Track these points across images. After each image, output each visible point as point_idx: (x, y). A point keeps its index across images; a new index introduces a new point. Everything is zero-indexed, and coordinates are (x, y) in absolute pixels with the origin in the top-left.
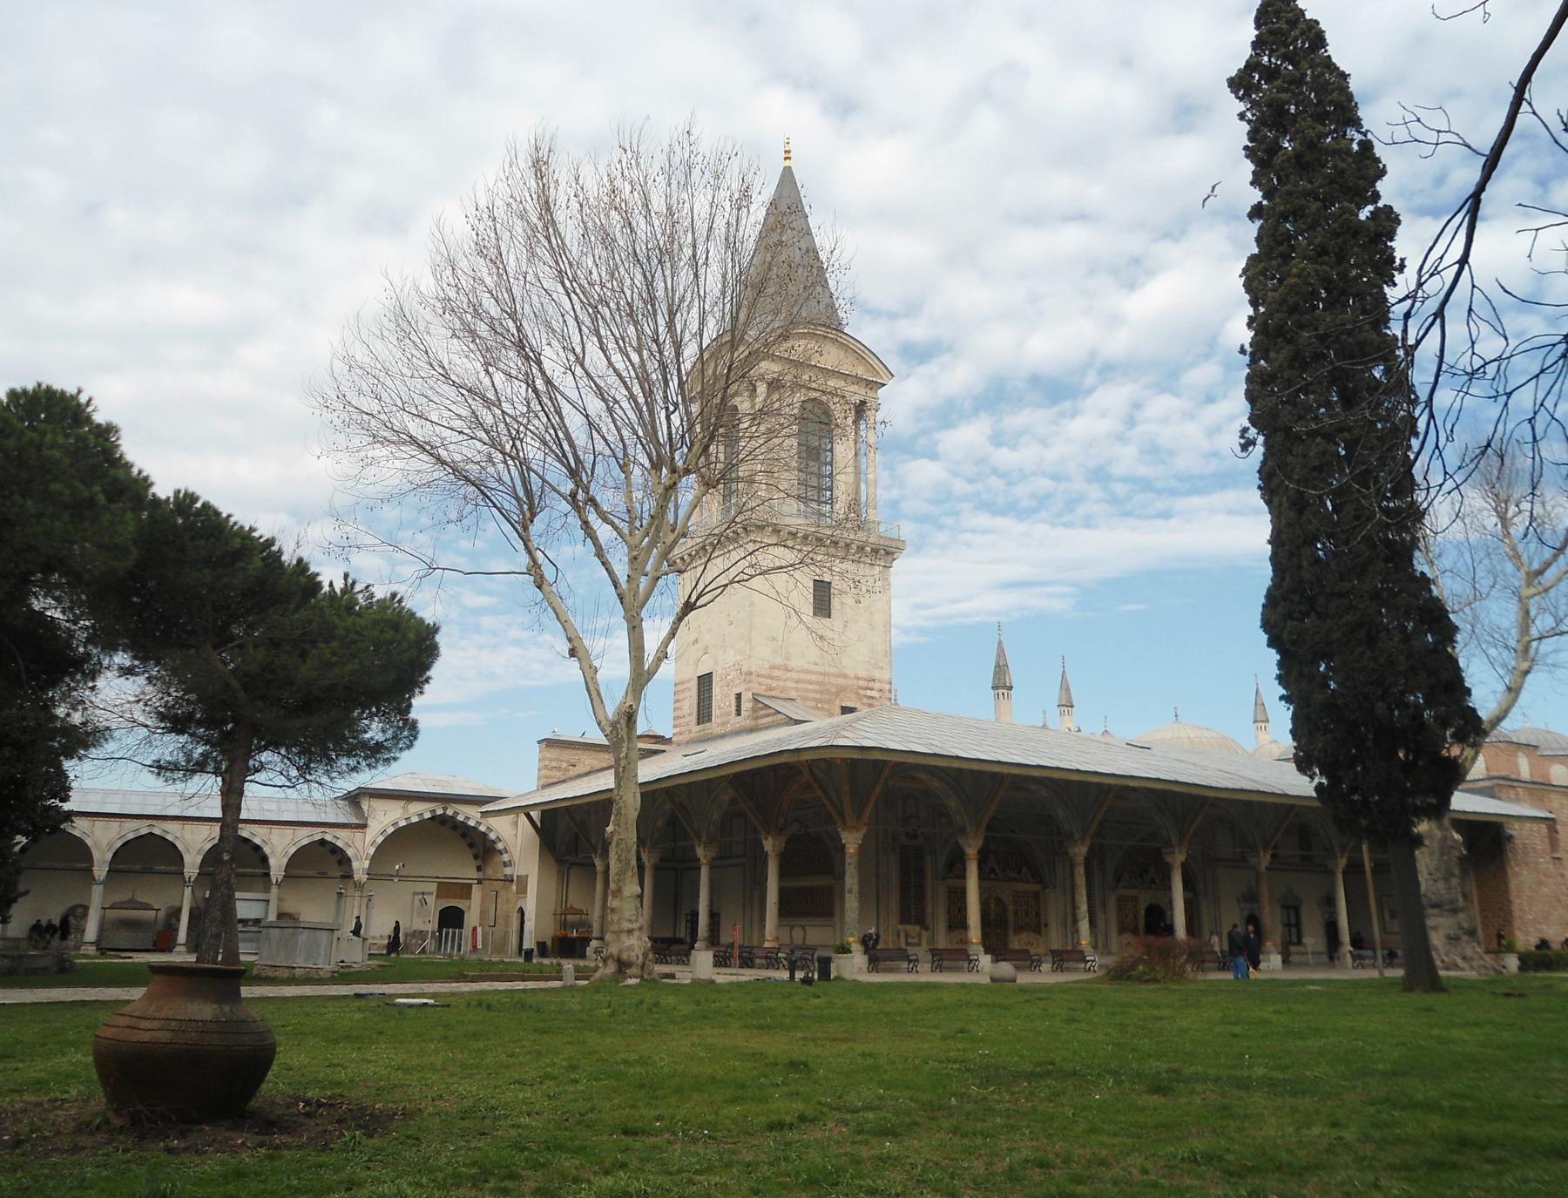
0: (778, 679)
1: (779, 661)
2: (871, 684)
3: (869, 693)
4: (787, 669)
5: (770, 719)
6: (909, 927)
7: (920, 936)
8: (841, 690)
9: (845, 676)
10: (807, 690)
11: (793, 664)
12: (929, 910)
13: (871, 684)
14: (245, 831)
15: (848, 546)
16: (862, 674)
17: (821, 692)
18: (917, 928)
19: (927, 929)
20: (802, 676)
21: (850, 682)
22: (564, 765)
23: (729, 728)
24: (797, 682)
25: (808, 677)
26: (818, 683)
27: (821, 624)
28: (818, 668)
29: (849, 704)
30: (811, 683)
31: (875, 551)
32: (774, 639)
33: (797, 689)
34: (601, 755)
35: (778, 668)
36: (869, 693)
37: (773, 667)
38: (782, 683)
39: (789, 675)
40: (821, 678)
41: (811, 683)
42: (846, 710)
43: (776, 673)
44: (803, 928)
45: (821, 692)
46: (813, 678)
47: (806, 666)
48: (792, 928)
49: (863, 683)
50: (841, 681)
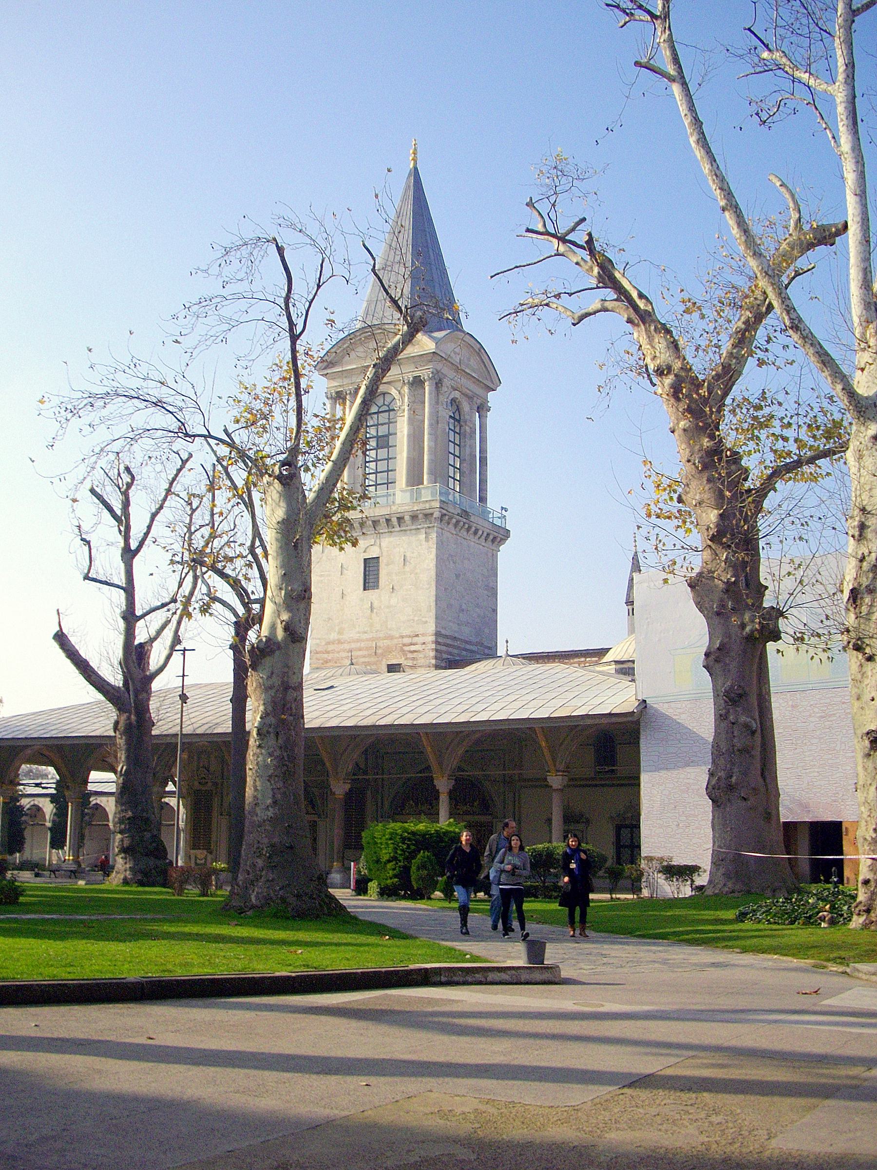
0: (333, 651)
2: (415, 640)
3: (413, 648)
4: (340, 642)
6: (198, 852)
7: (206, 858)
8: (388, 650)
9: (391, 638)
11: (345, 637)
12: (214, 838)
13: (415, 640)
14: (93, 800)
15: (388, 521)
17: (369, 656)
18: (205, 852)
19: (211, 853)
20: (353, 646)
21: (395, 641)
28: (365, 636)
29: (394, 662)
31: (414, 517)
32: (329, 619)
36: (413, 648)
39: (342, 647)
42: (393, 668)
43: (331, 648)
45: (369, 656)
46: (362, 645)
47: (356, 636)
49: (407, 641)
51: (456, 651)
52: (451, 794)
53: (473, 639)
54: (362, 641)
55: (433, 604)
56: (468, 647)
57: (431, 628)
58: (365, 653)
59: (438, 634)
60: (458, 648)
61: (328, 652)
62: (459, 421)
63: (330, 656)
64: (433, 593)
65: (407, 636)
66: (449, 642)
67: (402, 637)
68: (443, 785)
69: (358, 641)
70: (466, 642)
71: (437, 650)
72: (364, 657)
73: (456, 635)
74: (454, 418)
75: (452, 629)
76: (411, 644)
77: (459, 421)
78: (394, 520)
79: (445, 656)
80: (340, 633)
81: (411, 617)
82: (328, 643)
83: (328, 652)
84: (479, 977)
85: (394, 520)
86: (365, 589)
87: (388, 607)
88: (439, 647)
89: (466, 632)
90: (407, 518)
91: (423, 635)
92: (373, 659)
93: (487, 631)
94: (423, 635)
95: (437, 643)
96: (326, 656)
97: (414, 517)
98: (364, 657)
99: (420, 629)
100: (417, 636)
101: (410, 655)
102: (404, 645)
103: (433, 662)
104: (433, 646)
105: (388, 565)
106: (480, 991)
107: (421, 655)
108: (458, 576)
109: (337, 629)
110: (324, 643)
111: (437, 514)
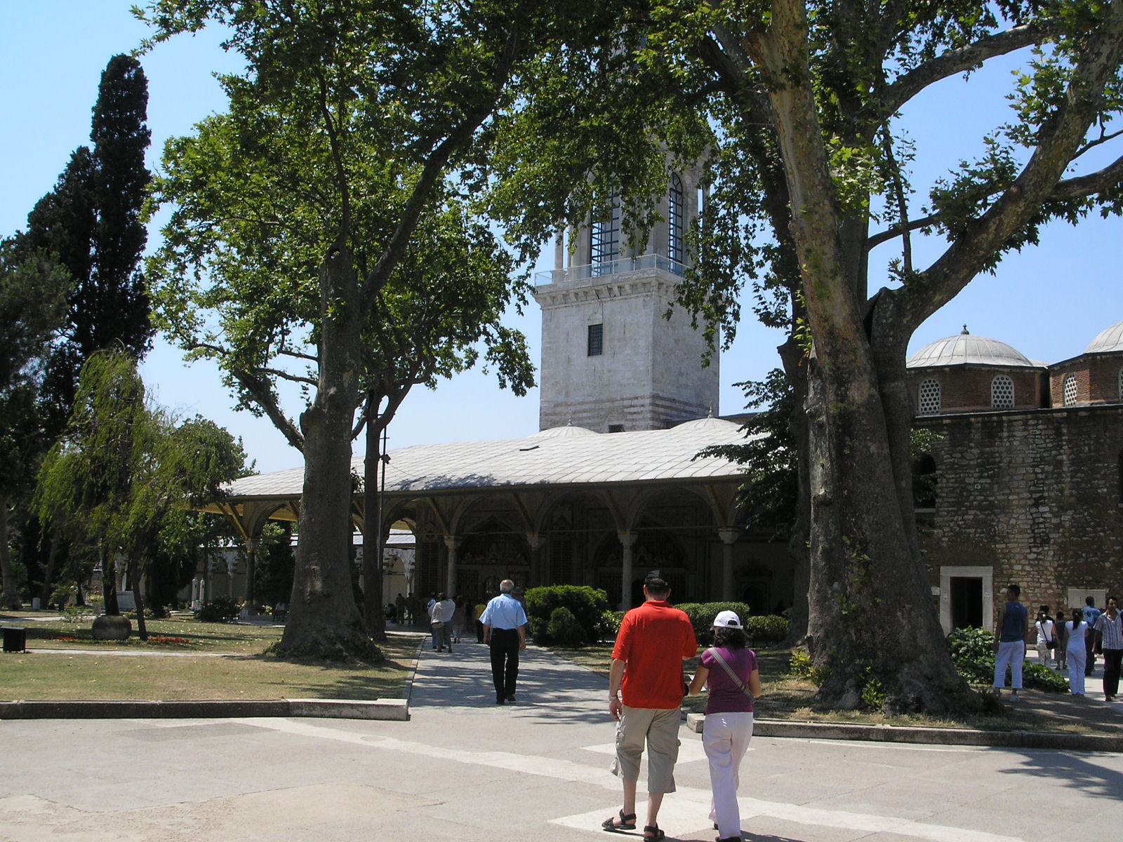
1: (561, 399)
3: (632, 410)
4: (567, 405)
9: (612, 401)
16: (628, 394)
17: (593, 417)
20: (579, 408)
21: (616, 404)
25: (583, 407)
26: (591, 410)
27: (596, 360)
28: (591, 399)
29: (616, 423)
30: (585, 411)
36: (632, 410)
37: (557, 405)
40: (592, 406)
41: (585, 411)
45: (593, 417)
49: (626, 403)
50: (608, 405)
51: (674, 412)
52: (634, 548)
53: (693, 401)
54: (587, 403)
55: (650, 368)
56: (687, 408)
57: (647, 390)
58: (589, 414)
59: (655, 397)
60: (676, 409)
62: (681, 194)
64: (650, 358)
65: (627, 399)
66: (668, 404)
68: (626, 539)
70: (686, 404)
71: (652, 411)
72: (589, 418)
73: (676, 397)
74: (676, 191)
75: (670, 392)
76: (631, 406)
77: (681, 194)
78: (616, 289)
79: (662, 417)
80: (567, 395)
81: (632, 381)
82: (557, 405)
83: (556, 414)
84: (334, 711)
85: (616, 289)
86: (589, 355)
87: (609, 371)
88: (656, 409)
89: (686, 395)
90: (627, 287)
91: (642, 397)
92: (596, 421)
93: (708, 393)
94: (642, 397)
95: (653, 404)
96: (554, 417)
97: (633, 286)
98: (589, 418)
99: (639, 392)
100: (637, 398)
101: (629, 417)
103: (651, 423)
104: (651, 408)
105: (610, 331)
106: (315, 725)
107: (640, 416)
108: (677, 341)
111: (654, 283)
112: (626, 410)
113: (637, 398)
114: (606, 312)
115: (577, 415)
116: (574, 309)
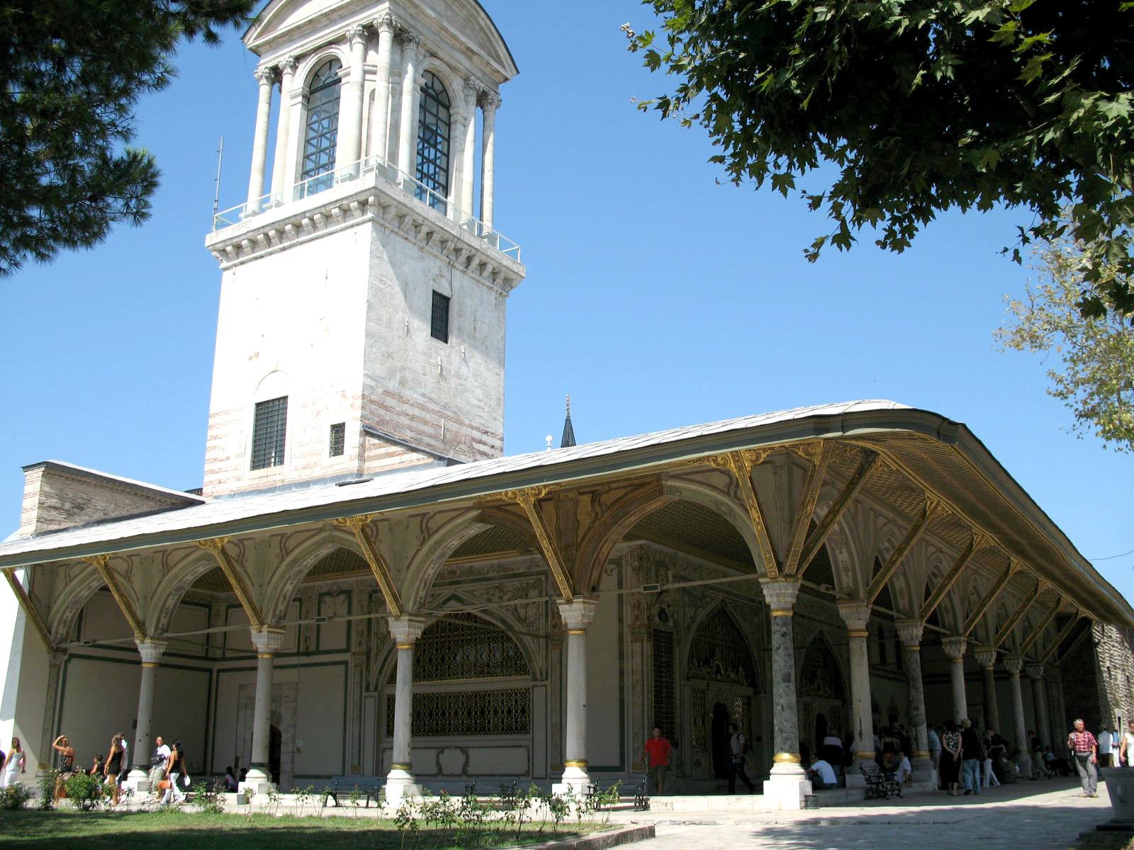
1: (392, 385)
2: (484, 438)
4: (400, 398)
5: (395, 460)
10: (421, 433)
13: (484, 438)
21: (464, 430)
22: (68, 506)
23: (317, 473)
24: (413, 418)
30: (426, 422)
33: (411, 429)
34: (120, 498)
35: (393, 395)
37: (386, 393)
38: (396, 418)
41: (426, 422)
43: (390, 402)
44: (464, 750)
47: (421, 400)
48: (441, 750)
49: (476, 434)
61: (386, 408)
63: (388, 416)
65: (477, 429)
67: (472, 428)
69: (423, 408)
76: (480, 442)
80: (403, 383)
83: (386, 408)
100: (486, 433)
102: (474, 439)
105: (460, 316)
109: (398, 376)
110: (380, 391)
112: (476, 446)
113: (486, 433)
114: (456, 285)
115: (414, 424)
116: (415, 252)
